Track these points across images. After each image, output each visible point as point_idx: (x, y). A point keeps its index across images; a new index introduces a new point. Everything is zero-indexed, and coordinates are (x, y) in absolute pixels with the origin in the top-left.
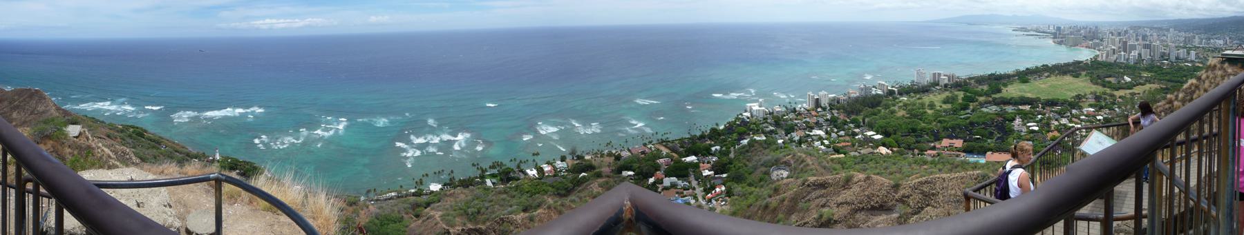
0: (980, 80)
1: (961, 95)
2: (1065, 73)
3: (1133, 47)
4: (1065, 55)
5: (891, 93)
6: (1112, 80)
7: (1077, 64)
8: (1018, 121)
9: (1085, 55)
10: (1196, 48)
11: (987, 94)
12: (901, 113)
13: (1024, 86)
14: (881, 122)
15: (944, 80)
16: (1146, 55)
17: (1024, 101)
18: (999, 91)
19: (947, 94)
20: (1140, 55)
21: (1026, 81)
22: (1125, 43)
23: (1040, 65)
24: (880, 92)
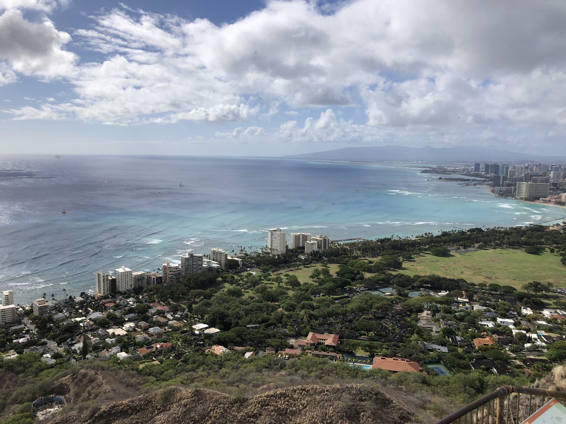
0: (368, 248)
1: (334, 269)
2: (513, 245)
5: (232, 265)
7: (538, 229)
8: (424, 314)
11: (377, 269)
12: (248, 294)
13: (442, 261)
14: (215, 308)
15: (312, 245)
17: (436, 284)
18: (398, 266)
19: (319, 267)
21: (445, 254)
23: (466, 227)
24: (215, 265)
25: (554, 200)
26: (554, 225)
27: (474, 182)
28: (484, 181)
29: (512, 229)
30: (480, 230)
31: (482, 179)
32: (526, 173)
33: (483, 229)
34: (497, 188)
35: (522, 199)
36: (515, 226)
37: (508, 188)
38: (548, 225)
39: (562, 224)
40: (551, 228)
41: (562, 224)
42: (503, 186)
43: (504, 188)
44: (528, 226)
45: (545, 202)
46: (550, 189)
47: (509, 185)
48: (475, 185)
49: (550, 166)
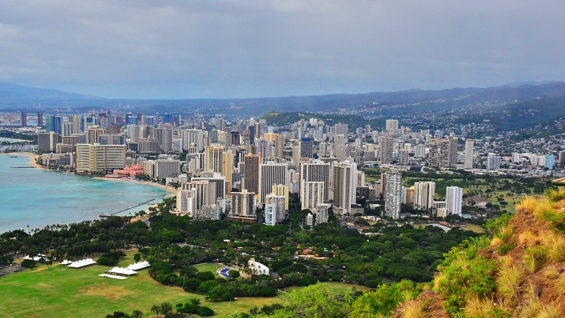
3: (276, 176)
4: (73, 203)
6: (219, 271)
7: (113, 224)
9: (134, 200)
10: (465, 178)
16: (315, 202)
20: (295, 198)
22: (252, 164)
25: (134, 173)
26: (137, 215)
27: (5, 147)
28: (22, 144)
29: (74, 226)
30: (20, 234)
31: (20, 140)
32: (89, 127)
33: (27, 231)
34: (45, 156)
35: (85, 173)
36: (78, 222)
37: (63, 155)
38: (128, 215)
39: (148, 212)
40: (133, 220)
41: (148, 212)
42: (54, 152)
43: (56, 157)
44: (100, 219)
45: (121, 176)
46: (128, 155)
47: (64, 150)
48: (7, 151)
49: (124, 116)
